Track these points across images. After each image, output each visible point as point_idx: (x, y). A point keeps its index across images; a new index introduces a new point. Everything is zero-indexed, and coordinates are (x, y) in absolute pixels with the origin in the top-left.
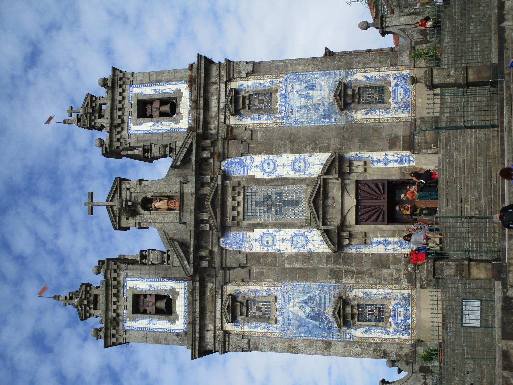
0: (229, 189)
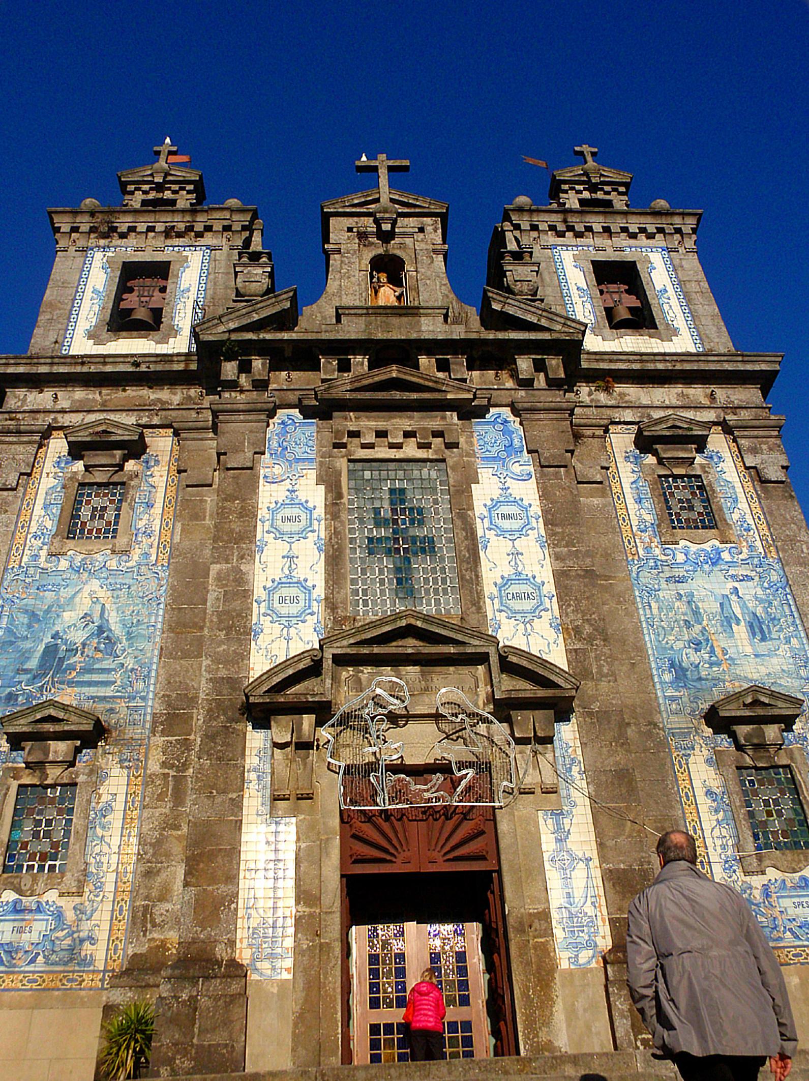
0: (434, 422)
